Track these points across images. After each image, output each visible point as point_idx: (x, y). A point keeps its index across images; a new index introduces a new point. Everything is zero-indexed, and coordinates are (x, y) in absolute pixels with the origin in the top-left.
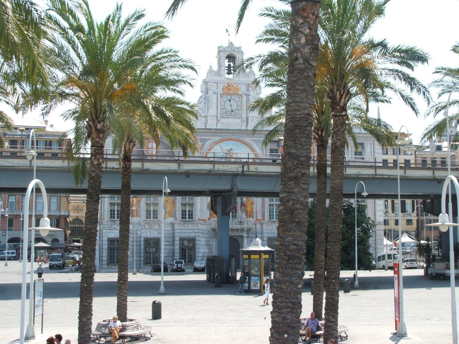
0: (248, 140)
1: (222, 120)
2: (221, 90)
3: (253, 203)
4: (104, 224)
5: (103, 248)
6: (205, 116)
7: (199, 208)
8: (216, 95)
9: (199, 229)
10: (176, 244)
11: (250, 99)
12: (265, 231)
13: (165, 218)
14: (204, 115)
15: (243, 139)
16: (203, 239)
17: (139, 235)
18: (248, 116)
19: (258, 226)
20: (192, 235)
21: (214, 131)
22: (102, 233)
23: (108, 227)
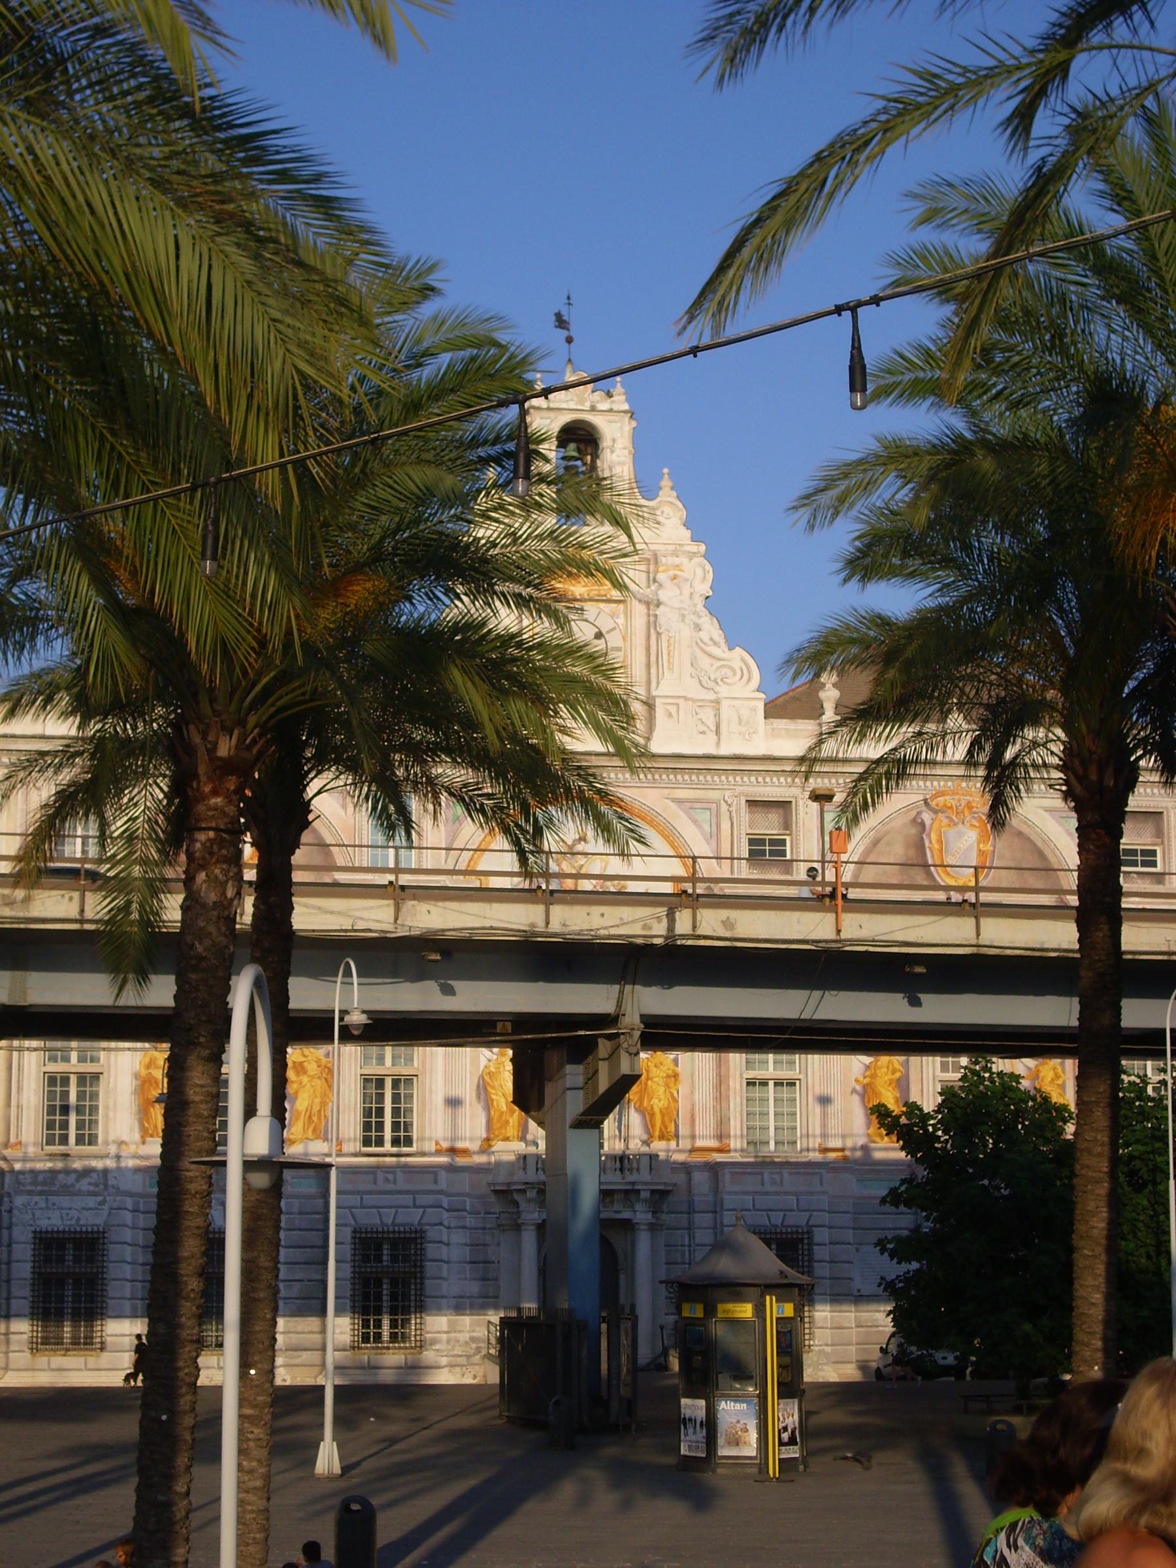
3: (676, 1076)
5: (14, 1275)
11: (661, 620)
12: (729, 1201)
16: (458, 1237)
18: (654, 693)
20: (412, 1217)
22: (10, 1211)
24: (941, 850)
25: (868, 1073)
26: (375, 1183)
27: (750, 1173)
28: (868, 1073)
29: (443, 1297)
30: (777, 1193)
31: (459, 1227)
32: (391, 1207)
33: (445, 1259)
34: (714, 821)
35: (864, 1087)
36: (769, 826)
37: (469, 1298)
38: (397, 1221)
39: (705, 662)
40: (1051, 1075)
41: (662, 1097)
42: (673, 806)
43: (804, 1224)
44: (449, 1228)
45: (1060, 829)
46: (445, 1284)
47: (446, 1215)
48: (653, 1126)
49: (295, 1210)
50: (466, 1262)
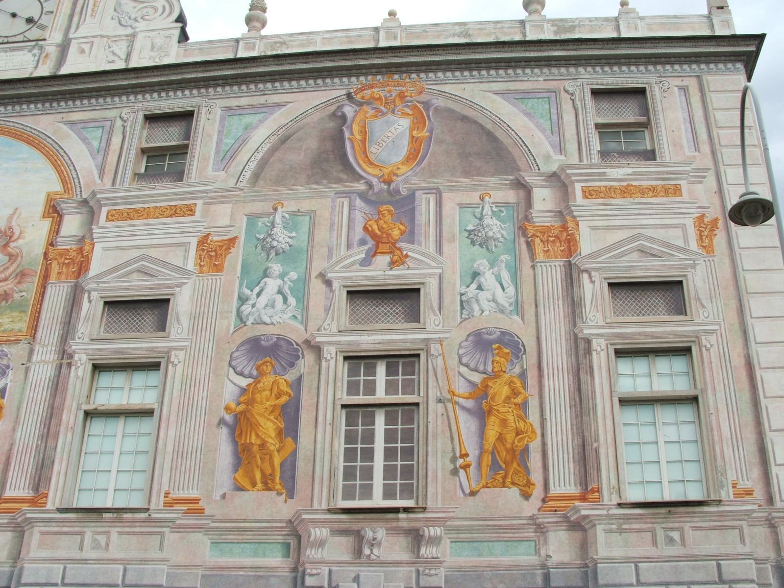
0: (46, 122)
15: (28, 122)
18: (71, 36)
24: (364, 141)
25: (242, 399)
27: (66, 533)
30: (99, 561)
34: (105, 137)
35: (238, 417)
36: (168, 136)
40: (505, 391)
42: (65, 128)
45: (515, 110)
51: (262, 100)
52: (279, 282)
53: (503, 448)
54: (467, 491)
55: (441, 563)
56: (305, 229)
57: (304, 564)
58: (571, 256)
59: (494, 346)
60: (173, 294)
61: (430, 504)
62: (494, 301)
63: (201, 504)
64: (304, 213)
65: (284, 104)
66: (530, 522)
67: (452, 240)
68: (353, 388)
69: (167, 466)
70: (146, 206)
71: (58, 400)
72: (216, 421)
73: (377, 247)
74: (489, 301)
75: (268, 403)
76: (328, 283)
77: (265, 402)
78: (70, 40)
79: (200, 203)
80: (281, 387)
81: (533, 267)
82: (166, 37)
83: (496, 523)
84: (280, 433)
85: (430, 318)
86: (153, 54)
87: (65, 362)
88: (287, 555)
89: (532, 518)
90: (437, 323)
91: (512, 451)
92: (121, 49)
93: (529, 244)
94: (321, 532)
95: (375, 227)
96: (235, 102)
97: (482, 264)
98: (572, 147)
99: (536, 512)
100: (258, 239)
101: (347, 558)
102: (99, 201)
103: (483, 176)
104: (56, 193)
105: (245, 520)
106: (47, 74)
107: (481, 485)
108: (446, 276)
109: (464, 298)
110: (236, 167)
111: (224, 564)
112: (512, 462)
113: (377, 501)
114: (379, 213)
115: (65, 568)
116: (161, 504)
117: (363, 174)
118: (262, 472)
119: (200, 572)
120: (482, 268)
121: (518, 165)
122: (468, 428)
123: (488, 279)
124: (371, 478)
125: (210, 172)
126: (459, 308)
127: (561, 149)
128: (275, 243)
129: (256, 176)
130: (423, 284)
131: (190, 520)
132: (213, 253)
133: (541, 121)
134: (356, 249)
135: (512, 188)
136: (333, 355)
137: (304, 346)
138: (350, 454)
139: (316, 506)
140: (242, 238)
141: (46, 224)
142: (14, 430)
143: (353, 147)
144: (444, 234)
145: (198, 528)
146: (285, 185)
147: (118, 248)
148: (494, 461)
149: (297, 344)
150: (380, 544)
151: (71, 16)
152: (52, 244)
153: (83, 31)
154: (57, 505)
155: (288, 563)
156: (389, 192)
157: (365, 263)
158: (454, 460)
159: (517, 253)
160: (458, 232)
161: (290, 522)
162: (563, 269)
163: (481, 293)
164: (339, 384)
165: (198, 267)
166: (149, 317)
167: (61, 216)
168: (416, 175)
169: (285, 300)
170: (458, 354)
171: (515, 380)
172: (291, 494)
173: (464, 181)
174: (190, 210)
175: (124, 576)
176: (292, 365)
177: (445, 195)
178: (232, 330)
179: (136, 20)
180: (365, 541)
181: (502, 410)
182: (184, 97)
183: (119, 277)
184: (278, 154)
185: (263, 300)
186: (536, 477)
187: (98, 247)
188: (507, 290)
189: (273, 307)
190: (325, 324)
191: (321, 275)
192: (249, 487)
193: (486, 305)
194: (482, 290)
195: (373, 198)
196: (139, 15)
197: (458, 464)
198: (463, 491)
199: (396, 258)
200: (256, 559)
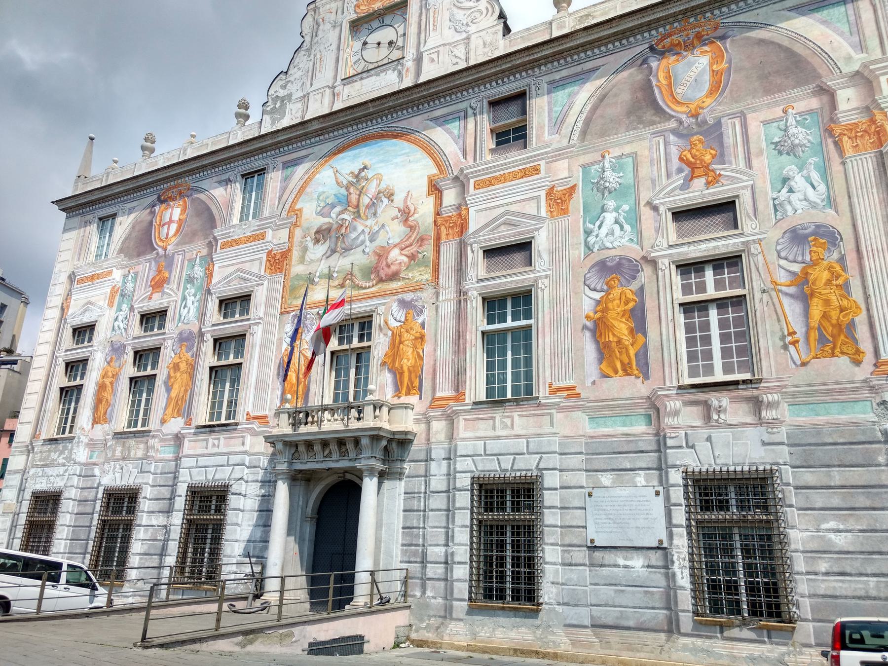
1: (347, 89)
2: (352, 10)
3: (422, 338)
4: (36, 449)
6: (304, 96)
7: (253, 379)
8: (338, 29)
9: (245, 453)
10: (177, 507)
13: (163, 422)
14: (302, 95)
15: (403, 124)
17: (97, 481)
19: (439, 427)
21: (316, 126)
23: (40, 460)
24: (670, 85)
25: (598, 308)
26: (207, 448)
27: (482, 419)
28: (598, 308)
29: (236, 541)
30: (508, 437)
31: (253, 481)
32: (213, 466)
33: (241, 508)
35: (596, 323)
37: (254, 541)
38: (216, 478)
39: (460, 15)
40: (826, 275)
41: (411, 357)
43: (534, 468)
44: (247, 482)
46: (238, 528)
47: (246, 471)
48: (402, 383)
49: (159, 471)
50: (254, 511)
51: (578, 69)
52: (615, 214)
53: (828, 324)
54: (799, 363)
55: (781, 423)
56: (630, 168)
57: (664, 429)
58: (882, 146)
59: (810, 239)
60: (533, 237)
61: (765, 376)
62: (805, 200)
63: (577, 390)
64: (628, 156)
65: (597, 68)
66: (863, 384)
67: (760, 153)
68: (687, 290)
69: (548, 364)
70: (502, 173)
71: (461, 325)
72: (581, 327)
73: (693, 172)
74: (801, 201)
75: (619, 310)
76: (655, 209)
77: (616, 309)
78: (422, 53)
79: (542, 163)
80: (628, 296)
81: (843, 163)
82: (493, 34)
83: (830, 387)
84: (632, 331)
85: (747, 224)
86: (486, 50)
87: (462, 298)
88: (649, 423)
89: (865, 381)
90: (754, 226)
91: (839, 326)
92: (460, 51)
93: (836, 143)
94: (675, 404)
95: (689, 156)
96: (557, 76)
97: (791, 169)
98: (873, 42)
99: (869, 376)
100: (593, 183)
101: (699, 423)
102: (466, 175)
103: (785, 90)
104: (434, 175)
105: (613, 400)
106: (411, 85)
107: (811, 357)
108: (759, 185)
109: (776, 202)
110: (566, 130)
111: (600, 434)
112: (839, 335)
113: (720, 376)
114: (691, 143)
115: (485, 444)
116: (547, 393)
117: (673, 113)
118: (621, 361)
119: (583, 440)
120: (791, 173)
121: (819, 73)
122: (793, 310)
123: (799, 182)
124: (711, 359)
125: (546, 137)
126: (773, 211)
127: (862, 47)
128: (607, 184)
129: (584, 133)
130: (738, 196)
131: (571, 403)
132: (559, 201)
133: (839, 25)
134: (675, 177)
135: (815, 96)
136: (667, 265)
137: (642, 262)
138: (691, 342)
139: (668, 384)
140: (580, 185)
141: (431, 200)
142: (435, 350)
143: (661, 92)
144: (752, 150)
145: (578, 408)
146: (608, 136)
147: (486, 209)
148: (821, 335)
149: (636, 261)
150: (725, 411)
151: (419, 34)
152: (438, 214)
153: (431, 43)
154: (473, 400)
155: (651, 429)
156: (697, 124)
157: (685, 186)
158: (783, 338)
159: (825, 153)
160: (765, 147)
161: (649, 398)
162: (874, 159)
163: (793, 195)
164: (674, 288)
165: (549, 213)
166: (518, 257)
167: (441, 192)
168: (720, 105)
169: (622, 228)
170: (776, 250)
171: (835, 265)
172: (646, 376)
173: (767, 99)
174: (537, 170)
175: (527, 446)
176: (634, 278)
177: (749, 116)
178: (583, 257)
179: (467, 25)
180: (712, 409)
181: (823, 292)
182: (516, 80)
183: (491, 231)
184: (599, 112)
185: (604, 231)
186: (866, 345)
187: (472, 211)
188: (818, 189)
189: (613, 234)
190: (657, 242)
191: (649, 204)
192: (612, 374)
193: (799, 205)
194: (793, 192)
195: (685, 132)
196: (469, 20)
197: (788, 341)
198: (795, 363)
199: (710, 179)
200: (625, 428)
